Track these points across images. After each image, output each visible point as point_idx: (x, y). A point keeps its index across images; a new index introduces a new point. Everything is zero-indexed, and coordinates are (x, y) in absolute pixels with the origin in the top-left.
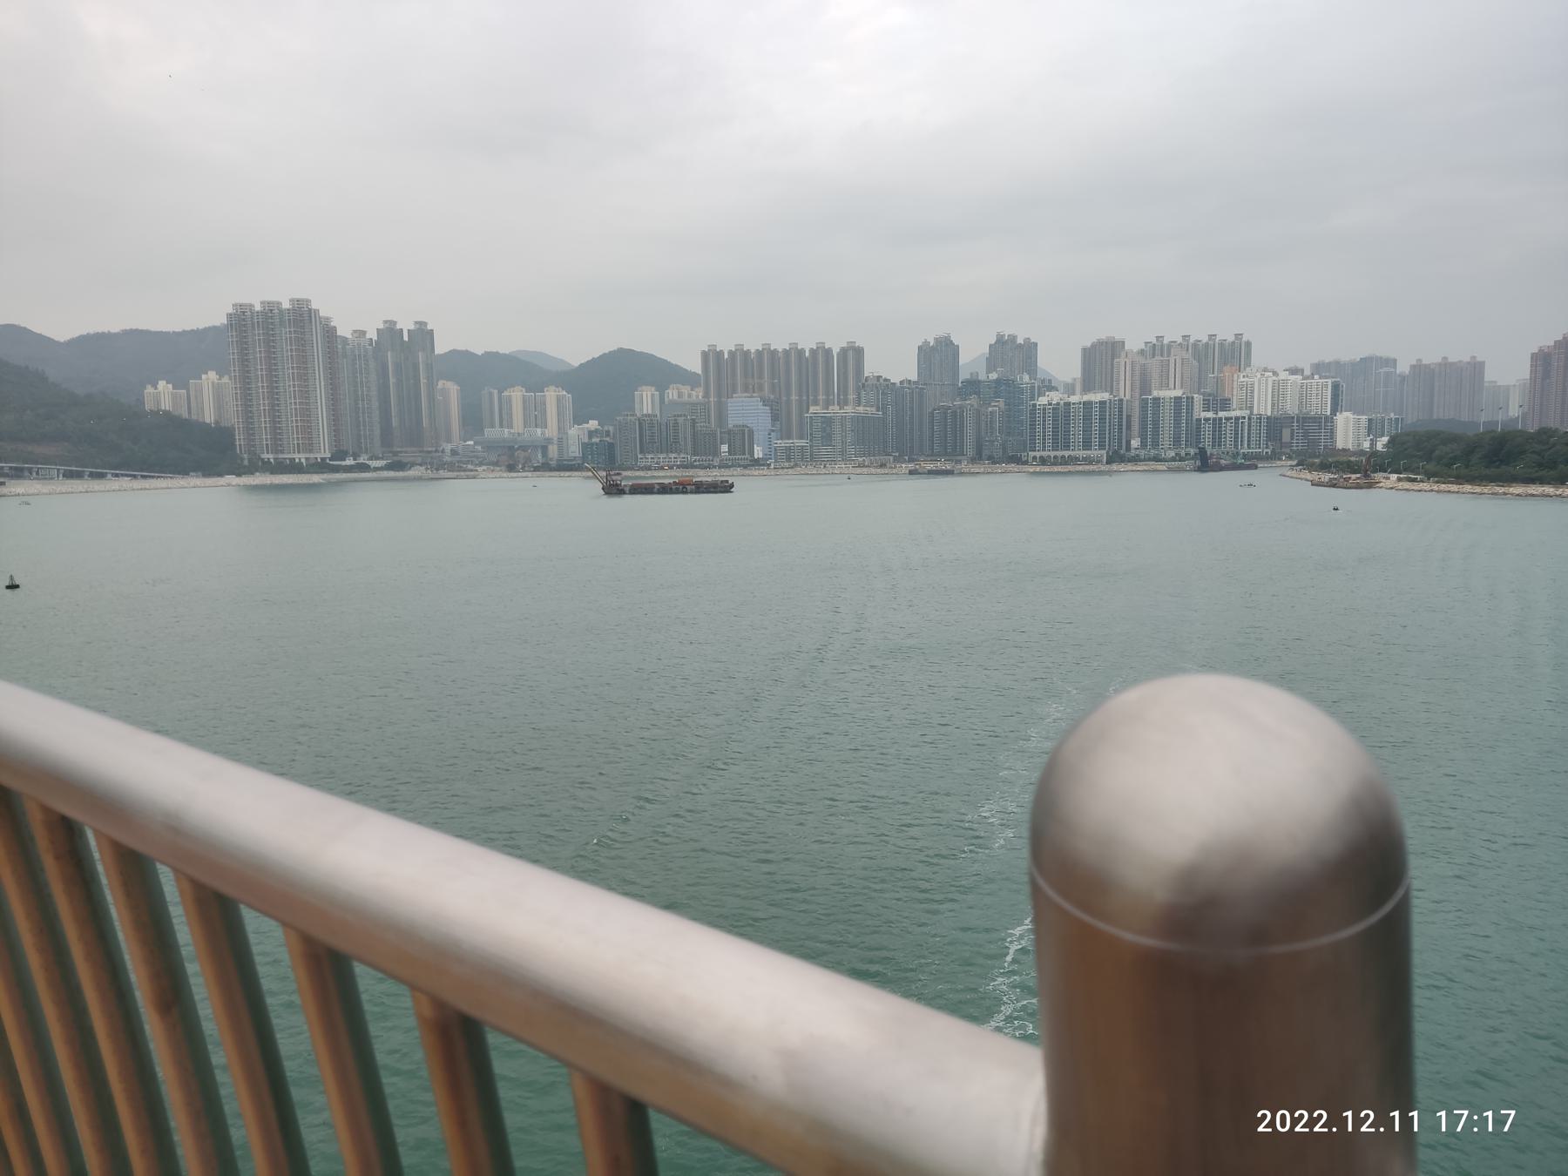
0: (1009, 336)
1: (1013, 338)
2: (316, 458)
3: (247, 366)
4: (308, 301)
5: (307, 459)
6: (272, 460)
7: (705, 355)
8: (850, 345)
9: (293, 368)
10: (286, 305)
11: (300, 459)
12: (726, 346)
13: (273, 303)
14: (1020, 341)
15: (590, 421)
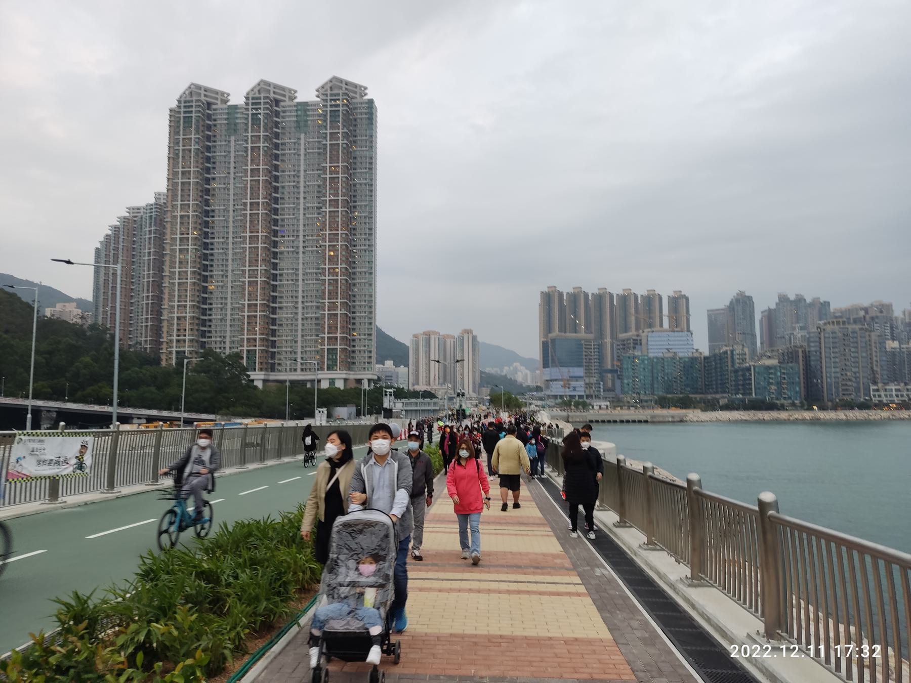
0: (797, 295)
1: (800, 300)
2: (359, 381)
3: (207, 203)
4: (360, 90)
5: (346, 380)
6: (259, 384)
7: (548, 299)
8: (679, 294)
9: (334, 203)
10: (307, 94)
11: (332, 381)
12: (566, 288)
13: (283, 89)
14: (808, 300)
15: (386, 362)
